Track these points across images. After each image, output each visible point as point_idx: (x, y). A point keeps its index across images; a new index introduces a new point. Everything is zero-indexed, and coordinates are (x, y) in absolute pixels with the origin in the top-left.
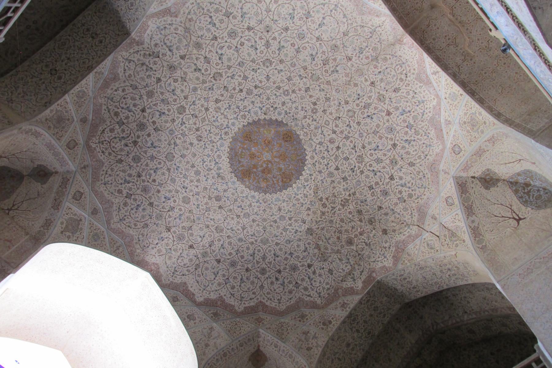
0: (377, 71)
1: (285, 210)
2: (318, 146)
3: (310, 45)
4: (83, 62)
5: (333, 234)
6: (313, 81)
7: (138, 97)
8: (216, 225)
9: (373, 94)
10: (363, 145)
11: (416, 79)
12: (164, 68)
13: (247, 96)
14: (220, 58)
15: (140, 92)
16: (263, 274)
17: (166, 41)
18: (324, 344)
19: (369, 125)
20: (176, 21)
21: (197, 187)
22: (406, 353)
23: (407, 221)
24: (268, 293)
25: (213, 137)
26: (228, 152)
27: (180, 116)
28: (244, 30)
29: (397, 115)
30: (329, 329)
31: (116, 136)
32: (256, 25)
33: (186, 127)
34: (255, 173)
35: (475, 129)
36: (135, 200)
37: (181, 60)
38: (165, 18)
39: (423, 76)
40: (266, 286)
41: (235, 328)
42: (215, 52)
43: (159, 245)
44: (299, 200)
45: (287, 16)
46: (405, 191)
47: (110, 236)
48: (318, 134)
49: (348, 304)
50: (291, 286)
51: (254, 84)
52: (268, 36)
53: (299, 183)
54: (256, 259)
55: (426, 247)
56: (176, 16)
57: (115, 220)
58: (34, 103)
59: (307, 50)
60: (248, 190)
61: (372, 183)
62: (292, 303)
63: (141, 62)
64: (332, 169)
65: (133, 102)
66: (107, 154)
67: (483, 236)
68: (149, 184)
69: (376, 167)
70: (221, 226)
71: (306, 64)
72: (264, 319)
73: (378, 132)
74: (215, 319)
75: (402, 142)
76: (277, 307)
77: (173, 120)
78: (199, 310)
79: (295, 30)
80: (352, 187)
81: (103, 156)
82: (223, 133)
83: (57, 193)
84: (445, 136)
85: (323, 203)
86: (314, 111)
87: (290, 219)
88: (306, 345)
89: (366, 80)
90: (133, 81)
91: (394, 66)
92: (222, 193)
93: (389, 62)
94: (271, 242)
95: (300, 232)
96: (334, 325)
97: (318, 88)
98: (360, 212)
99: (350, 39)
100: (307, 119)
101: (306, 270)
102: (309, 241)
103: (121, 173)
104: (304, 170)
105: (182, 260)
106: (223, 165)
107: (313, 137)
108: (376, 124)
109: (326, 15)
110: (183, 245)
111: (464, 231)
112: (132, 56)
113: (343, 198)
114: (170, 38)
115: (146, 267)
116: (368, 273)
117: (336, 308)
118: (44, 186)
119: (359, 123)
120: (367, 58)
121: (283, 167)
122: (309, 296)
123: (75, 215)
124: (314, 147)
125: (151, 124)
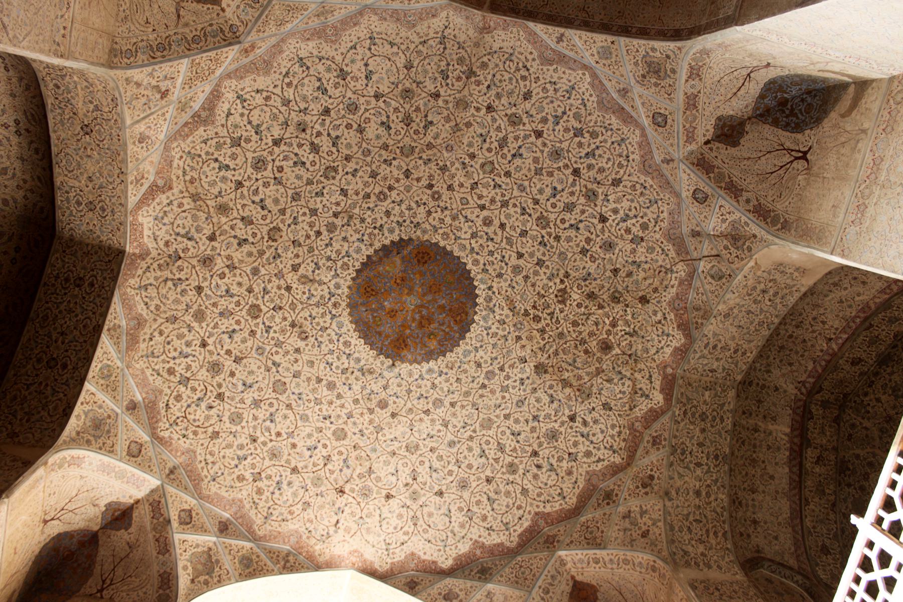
0: (483, 88)
1: (486, 362)
2: (473, 241)
3: (372, 111)
4: (84, 326)
6: (407, 157)
7: (185, 331)
8: (404, 444)
9: (499, 121)
10: (534, 199)
11: (542, 64)
12: (197, 268)
13: (331, 236)
14: (263, 208)
15: (184, 321)
16: (514, 472)
17: (177, 230)
18: (661, 513)
19: (523, 166)
20: (173, 195)
21: (342, 406)
22: (787, 453)
23: (663, 264)
24: (539, 495)
25: (321, 321)
26: (355, 331)
27: (258, 320)
28: (270, 149)
29: (551, 129)
30: (655, 487)
31: (189, 402)
32: (283, 132)
33: (275, 332)
34: (411, 335)
35: (662, 74)
36: (269, 477)
37: (213, 243)
38: (157, 200)
39: (549, 54)
40: (530, 487)
41: (523, 573)
42: (250, 203)
43: (341, 522)
44: (497, 333)
45: (316, 94)
46: (634, 225)
47: (265, 549)
48: (462, 225)
49: (660, 435)
50: (564, 464)
51: (331, 212)
52: (308, 137)
53: (481, 310)
54: (490, 457)
55: (713, 282)
56: (171, 188)
57: (259, 522)
58: (49, 420)
59: (372, 121)
60: (417, 366)
61: (581, 244)
62: (581, 486)
63: (161, 280)
64: (514, 261)
65: (183, 341)
66: (191, 436)
67: (774, 211)
68: (273, 443)
69: (571, 218)
70: (412, 442)
71: (384, 139)
72: (556, 536)
73: (541, 169)
74: (486, 579)
75: (582, 160)
76: (565, 506)
77: (253, 333)
78: (455, 580)
79: (338, 105)
80: (558, 267)
81: (188, 442)
82: (330, 308)
83: (154, 529)
84: (633, 114)
85: (532, 316)
86: (436, 196)
87: (502, 369)
88: (638, 532)
89: (478, 109)
90: (165, 312)
91: (501, 67)
92: (384, 393)
94: (496, 419)
95: (528, 378)
96: (659, 478)
97: (421, 162)
98: (591, 296)
99: (419, 69)
100: (434, 215)
101: (571, 428)
102: (548, 383)
103: (227, 451)
104: (476, 287)
105: (388, 523)
106: (359, 352)
107: (458, 234)
108: (531, 158)
109: (366, 59)
110: (376, 501)
111: (745, 222)
112: (144, 278)
113: (555, 292)
114: (179, 222)
115: (343, 564)
116: (659, 374)
117: (647, 453)
118: (132, 529)
119: (508, 174)
120: (459, 79)
121: (444, 302)
122: (599, 460)
123: (198, 546)
124: (468, 246)
125: (226, 356)
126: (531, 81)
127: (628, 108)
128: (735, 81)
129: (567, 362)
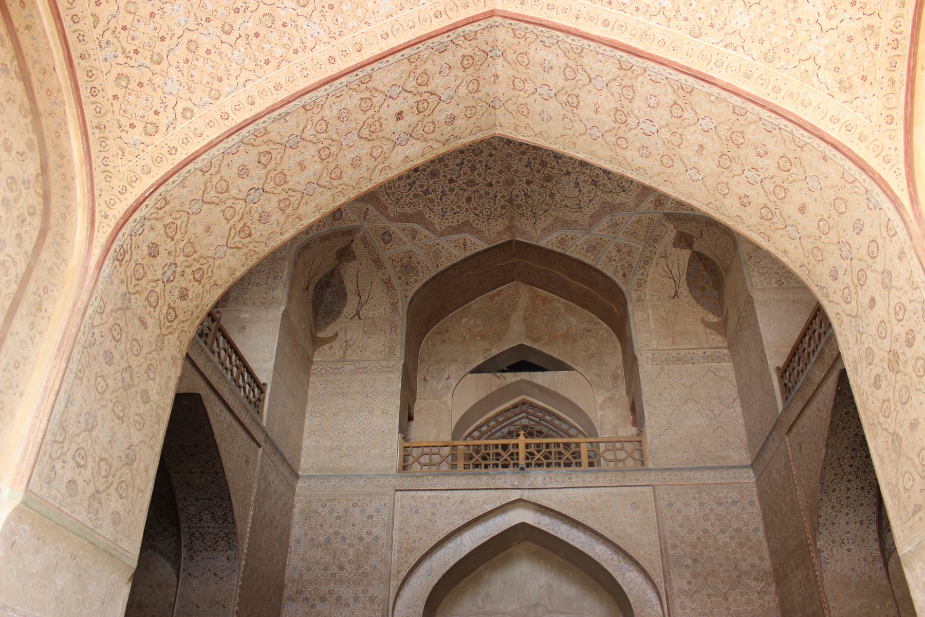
0: (499, 195)
84: (401, 225)
89: (498, 182)
93: (499, 209)
120: (517, 196)
127: (405, 225)
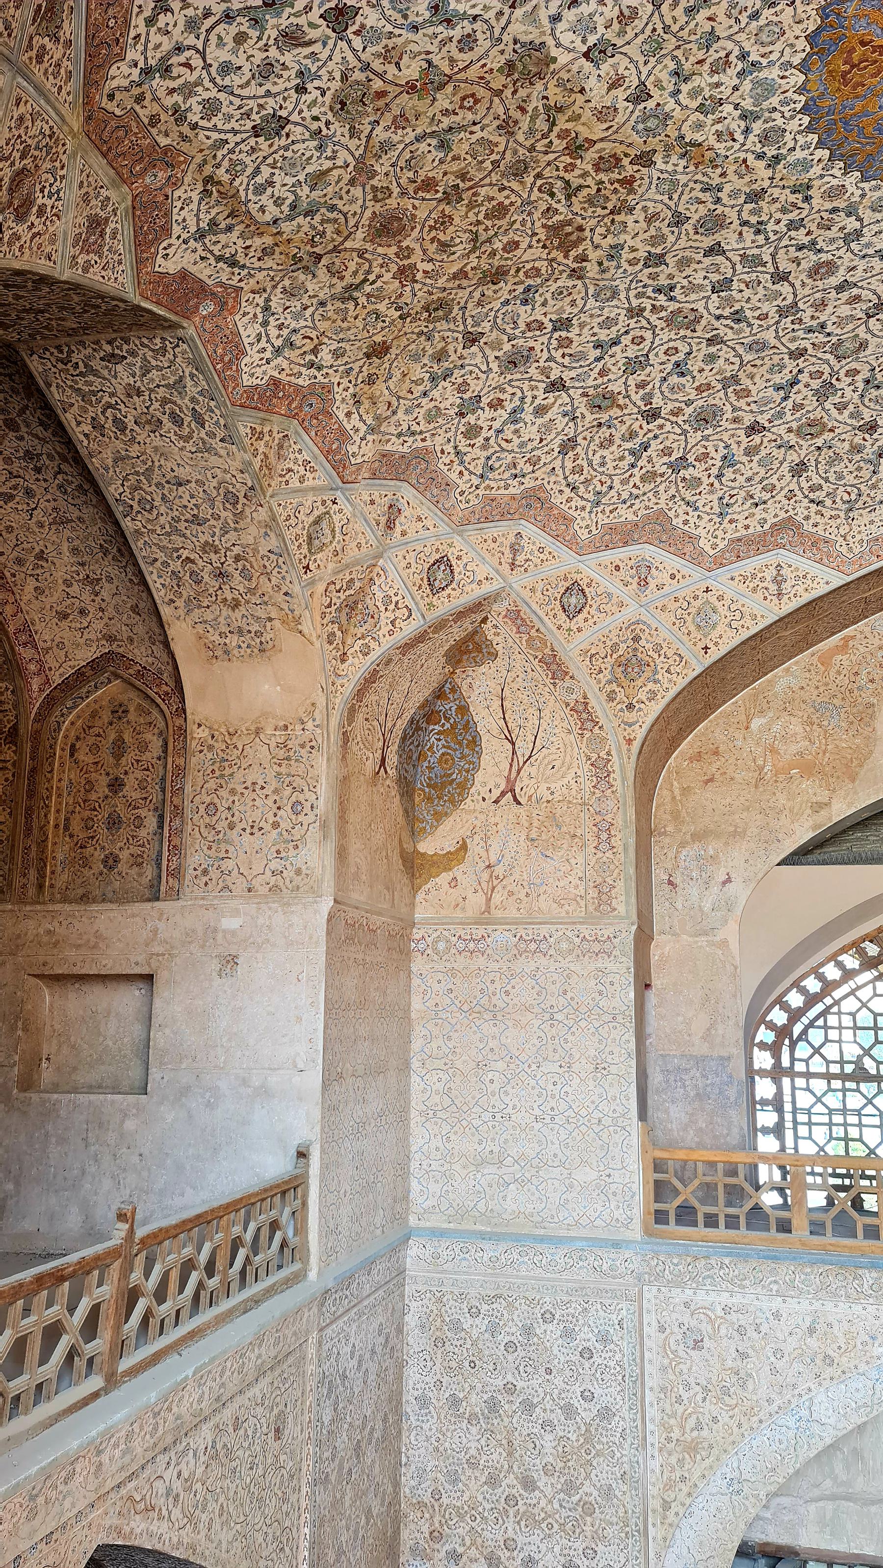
5: (455, 167)
29: (734, 446)
39: (785, 538)
44: (713, 72)
46: (493, 419)
55: (311, 519)
61: (577, 331)
75: (651, 435)
85: (626, 161)
95: (556, 19)
98: (496, 276)
102: (483, 43)
108: (754, 393)
113: (587, 233)
116: (221, 284)
126: (801, 489)
127: (619, 554)
128: (521, 722)
129: (462, 128)
